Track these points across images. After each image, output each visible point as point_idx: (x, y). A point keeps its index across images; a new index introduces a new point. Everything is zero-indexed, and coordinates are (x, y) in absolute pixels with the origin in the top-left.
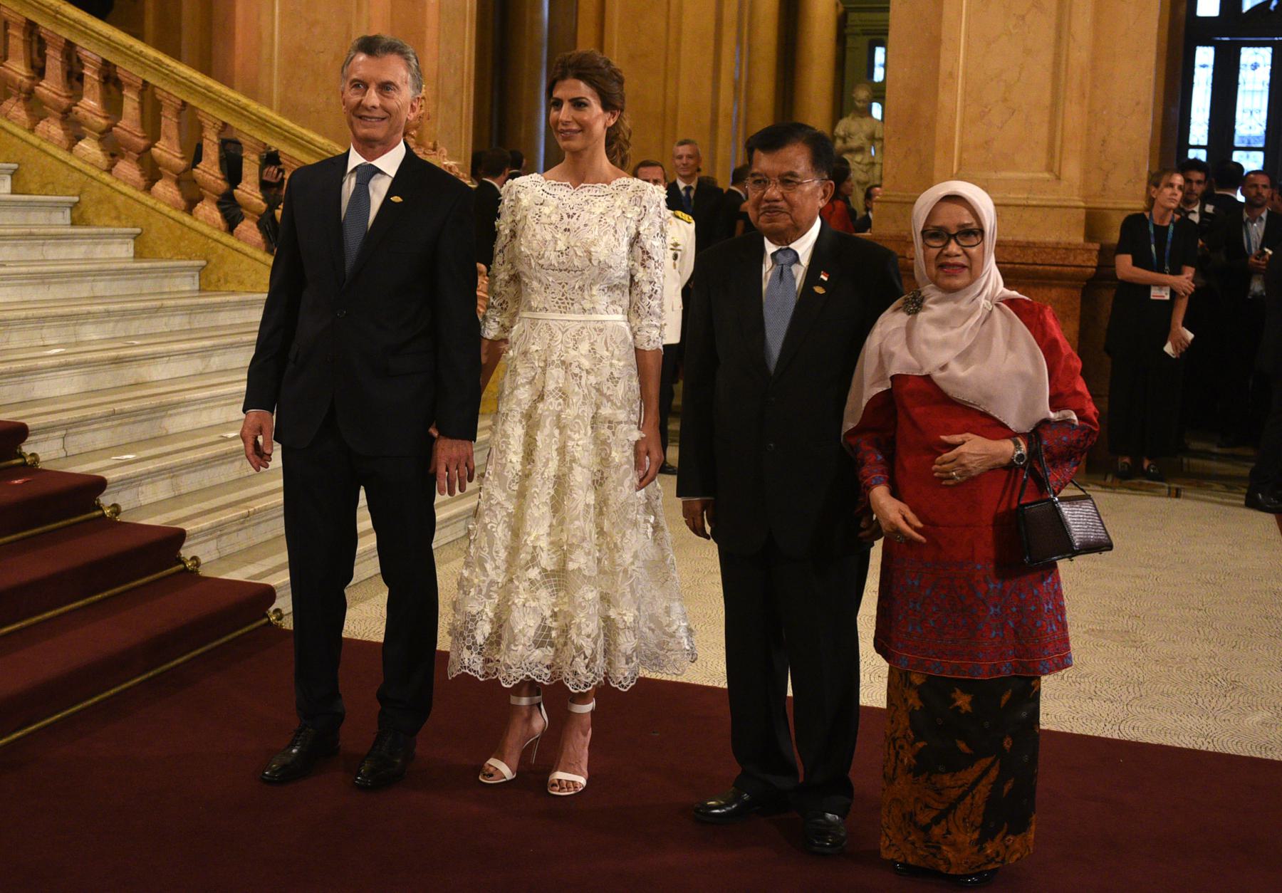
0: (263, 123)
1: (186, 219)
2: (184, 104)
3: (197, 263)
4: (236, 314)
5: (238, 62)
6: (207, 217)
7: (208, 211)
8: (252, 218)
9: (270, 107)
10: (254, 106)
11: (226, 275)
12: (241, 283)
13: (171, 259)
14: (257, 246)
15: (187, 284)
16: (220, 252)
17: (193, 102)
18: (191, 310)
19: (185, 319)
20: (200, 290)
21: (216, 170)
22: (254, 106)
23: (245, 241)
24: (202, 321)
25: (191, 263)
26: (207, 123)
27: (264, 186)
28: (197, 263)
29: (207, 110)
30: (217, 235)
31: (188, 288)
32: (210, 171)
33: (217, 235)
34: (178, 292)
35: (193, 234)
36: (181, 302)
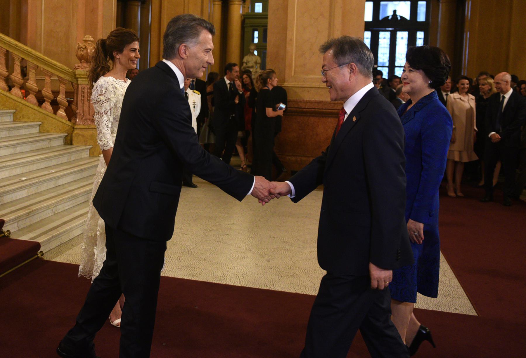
0: (37, 58)
1: (8, 94)
2: (7, 51)
3: (12, 111)
4: (27, 130)
5: (29, 35)
6: (16, 93)
7: (16, 91)
8: (33, 94)
9: (41, 53)
10: (33, 52)
11: (23, 115)
12: (29, 118)
13: (2, 109)
14: (35, 104)
15: (8, 119)
16: (21, 106)
17: (11, 50)
18: (9, 129)
19: (7, 132)
20: (13, 121)
21: (19, 76)
22: (33, 52)
23: (30, 102)
24: (14, 133)
25: (10, 111)
26: (16, 58)
27: (37, 81)
28: (12, 111)
29: (16, 53)
30: (19, 100)
31: (8, 120)
32: (16, 76)
33: (19, 100)
34: (5, 122)
35: (10, 100)
36: (5, 126)
